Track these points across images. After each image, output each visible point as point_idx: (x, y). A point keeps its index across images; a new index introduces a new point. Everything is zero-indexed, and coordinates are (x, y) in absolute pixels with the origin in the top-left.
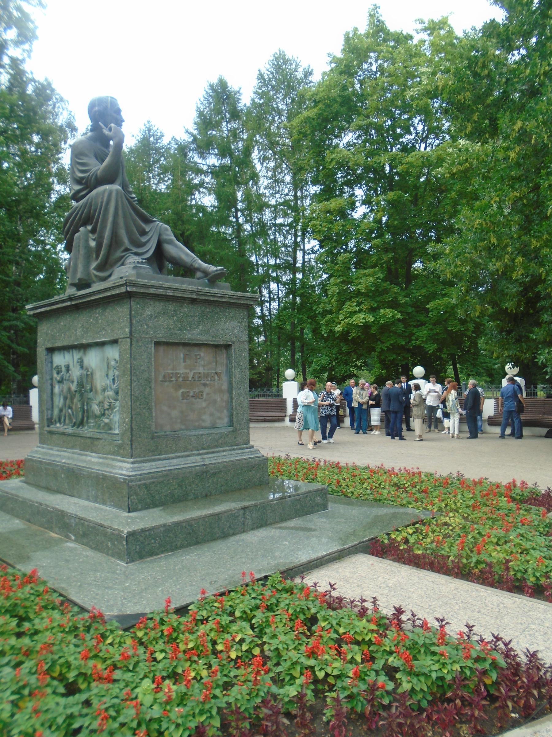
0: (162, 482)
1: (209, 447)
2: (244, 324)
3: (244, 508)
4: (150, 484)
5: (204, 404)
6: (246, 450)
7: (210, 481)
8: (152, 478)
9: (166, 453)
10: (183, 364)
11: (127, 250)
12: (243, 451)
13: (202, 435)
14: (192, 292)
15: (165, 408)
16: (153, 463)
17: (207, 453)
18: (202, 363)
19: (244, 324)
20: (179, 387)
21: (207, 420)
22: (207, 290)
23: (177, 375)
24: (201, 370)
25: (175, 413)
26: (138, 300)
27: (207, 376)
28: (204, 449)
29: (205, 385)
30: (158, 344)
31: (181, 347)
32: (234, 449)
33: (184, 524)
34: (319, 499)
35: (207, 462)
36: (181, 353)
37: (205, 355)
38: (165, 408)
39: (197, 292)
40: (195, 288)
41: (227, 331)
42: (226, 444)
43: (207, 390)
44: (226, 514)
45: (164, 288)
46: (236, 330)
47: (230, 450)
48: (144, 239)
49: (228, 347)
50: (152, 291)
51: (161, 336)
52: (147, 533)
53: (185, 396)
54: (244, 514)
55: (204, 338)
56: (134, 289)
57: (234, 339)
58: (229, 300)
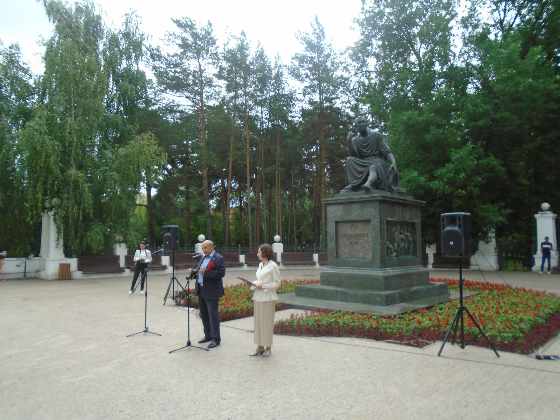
1: (359, 267)
2: (377, 209)
3: (337, 291)
5: (360, 248)
9: (340, 266)
10: (350, 230)
14: (346, 199)
15: (343, 248)
17: (357, 269)
18: (359, 229)
19: (377, 209)
20: (348, 240)
21: (361, 255)
22: (366, 196)
23: (348, 235)
24: (358, 232)
25: (347, 251)
27: (360, 235)
28: (356, 267)
29: (360, 239)
30: (337, 222)
34: (378, 299)
35: (354, 273)
38: (343, 248)
39: (349, 199)
40: (347, 198)
42: (368, 267)
43: (361, 241)
48: (360, 176)
50: (331, 202)
51: (338, 219)
53: (351, 243)
55: (356, 218)
56: (325, 203)
57: (371, 217)
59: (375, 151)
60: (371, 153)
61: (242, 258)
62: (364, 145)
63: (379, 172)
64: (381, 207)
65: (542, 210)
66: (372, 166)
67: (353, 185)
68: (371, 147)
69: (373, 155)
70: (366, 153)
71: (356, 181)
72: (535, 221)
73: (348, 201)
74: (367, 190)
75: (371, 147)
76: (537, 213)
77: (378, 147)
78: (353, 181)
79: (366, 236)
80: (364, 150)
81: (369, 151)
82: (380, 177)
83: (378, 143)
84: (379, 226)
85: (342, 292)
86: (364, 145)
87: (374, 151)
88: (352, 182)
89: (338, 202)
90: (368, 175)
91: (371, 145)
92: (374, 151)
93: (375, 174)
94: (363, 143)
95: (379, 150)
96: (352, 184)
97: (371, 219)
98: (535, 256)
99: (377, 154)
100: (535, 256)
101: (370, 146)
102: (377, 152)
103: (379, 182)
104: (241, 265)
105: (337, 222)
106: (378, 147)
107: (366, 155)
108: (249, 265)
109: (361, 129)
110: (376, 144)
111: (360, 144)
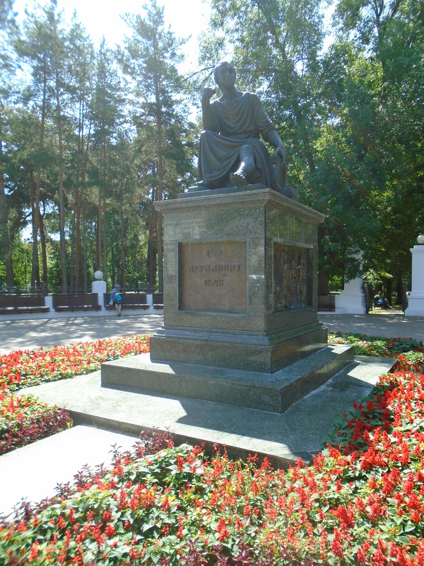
2: (259, 219)
13: (215, 316)
24: (222, 263)
29: (224, 275)
41: (241, 228)
45: (178, 203)
53: (206, 283)
61: (49, 301)
64: (267, 215)
66: (244, 146)
67: (212, 179)
79: (236, 269)
81: (239, 124)
82: (260, 166)
87: (246, 125)
89: (184, 205)
92: (246, 125)
93: (252, 160)
102: (252, 128)
104: (46, 310)
107: (233, 131)
108: (58, 310)
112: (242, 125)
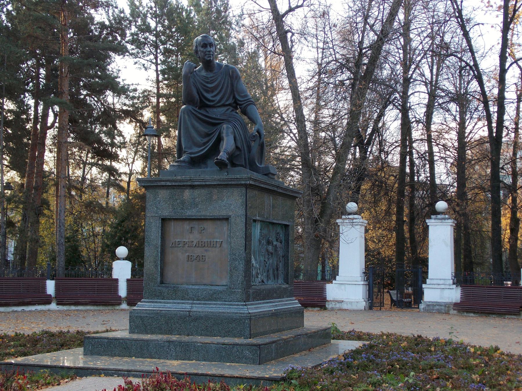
0: (153, 317)
3: (169, 342)
4: (144, 317)
6: (235, 307)
7: (192, 324)
8: (146, 313)
11: (185, 152)
12: (231, 307)
16: (153, 304)
26: (151, 190)
28: (198, 300)
30: (164, 220)
31: (188, 222)
32: (225, 304)
33: (121, 341)
34: (247, 353)
35: (195, 309)
36: (187, 226)
37: (209, 226)
41: (224, 208)
42: (220, 299)
44: (153, 342)
46: (232, 207)
47: (222, 304)
48: (205, 140)
49: (227, 219)
51: (166, 213)
52: (96, 340)
54: (169, 346)
57: (230, 214)
58: (220, 183)
59: (227, 100)
60: (219, 101)
62: (209, 86)
63: (237, 135)
65: (436, 213)
67: (193, 156)
68: (220, 91)
69: (224, 105)
70: (213, 101)
71: (196, 149)
72: (426, 229)
73: (189, 183)
74: (221, 165)
75: (220, 91)
76: (430, 218)
77: (232, 91)
78: (190, 148)
79: (218, 245)
80: (209, 96)
81: (218, 98)
82: (239, 145)
83: (232, 85)
84: (244, 229)
85: (180, 342)
86: (209, 86)
88: (190, 151)
89: (169, 184)
90: (219, 139)
91: (222, 88)
94: (207, 83)
95: (234, 97)
96: (191, 153)
97: (230, 216)
98: (424, 286)
99: (229, 105)
100: (424, 286)
101: (219, 89)
102: (231, 101)
103: (238, 153)
105: (164, 220)
106: (232, 91)
107: (212, 104)
109: (206, 58)
110: (229, 86)
111: (202, 83)
112: (221, 99)
